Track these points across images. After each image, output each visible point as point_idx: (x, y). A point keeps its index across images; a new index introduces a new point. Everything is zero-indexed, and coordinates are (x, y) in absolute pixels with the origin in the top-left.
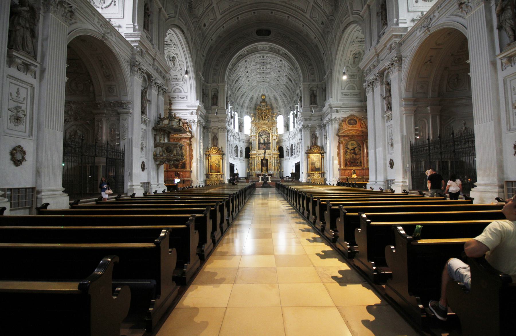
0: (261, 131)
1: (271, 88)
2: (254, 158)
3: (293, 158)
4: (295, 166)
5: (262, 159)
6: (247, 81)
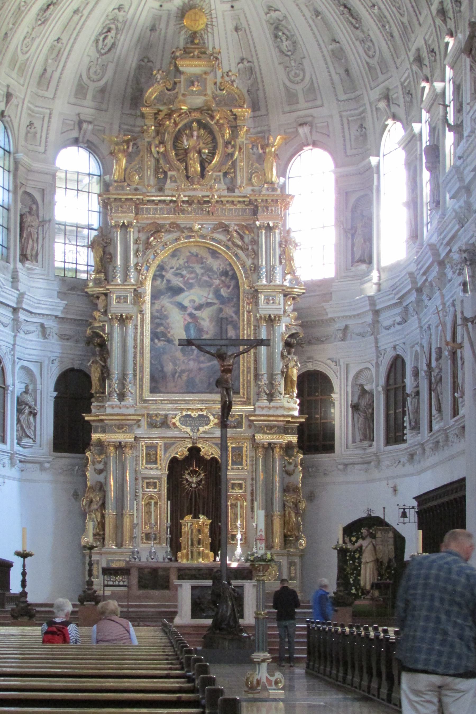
0: (174, 255)
2: (120, 447)
3: (404, 459)
4: (419, 513)
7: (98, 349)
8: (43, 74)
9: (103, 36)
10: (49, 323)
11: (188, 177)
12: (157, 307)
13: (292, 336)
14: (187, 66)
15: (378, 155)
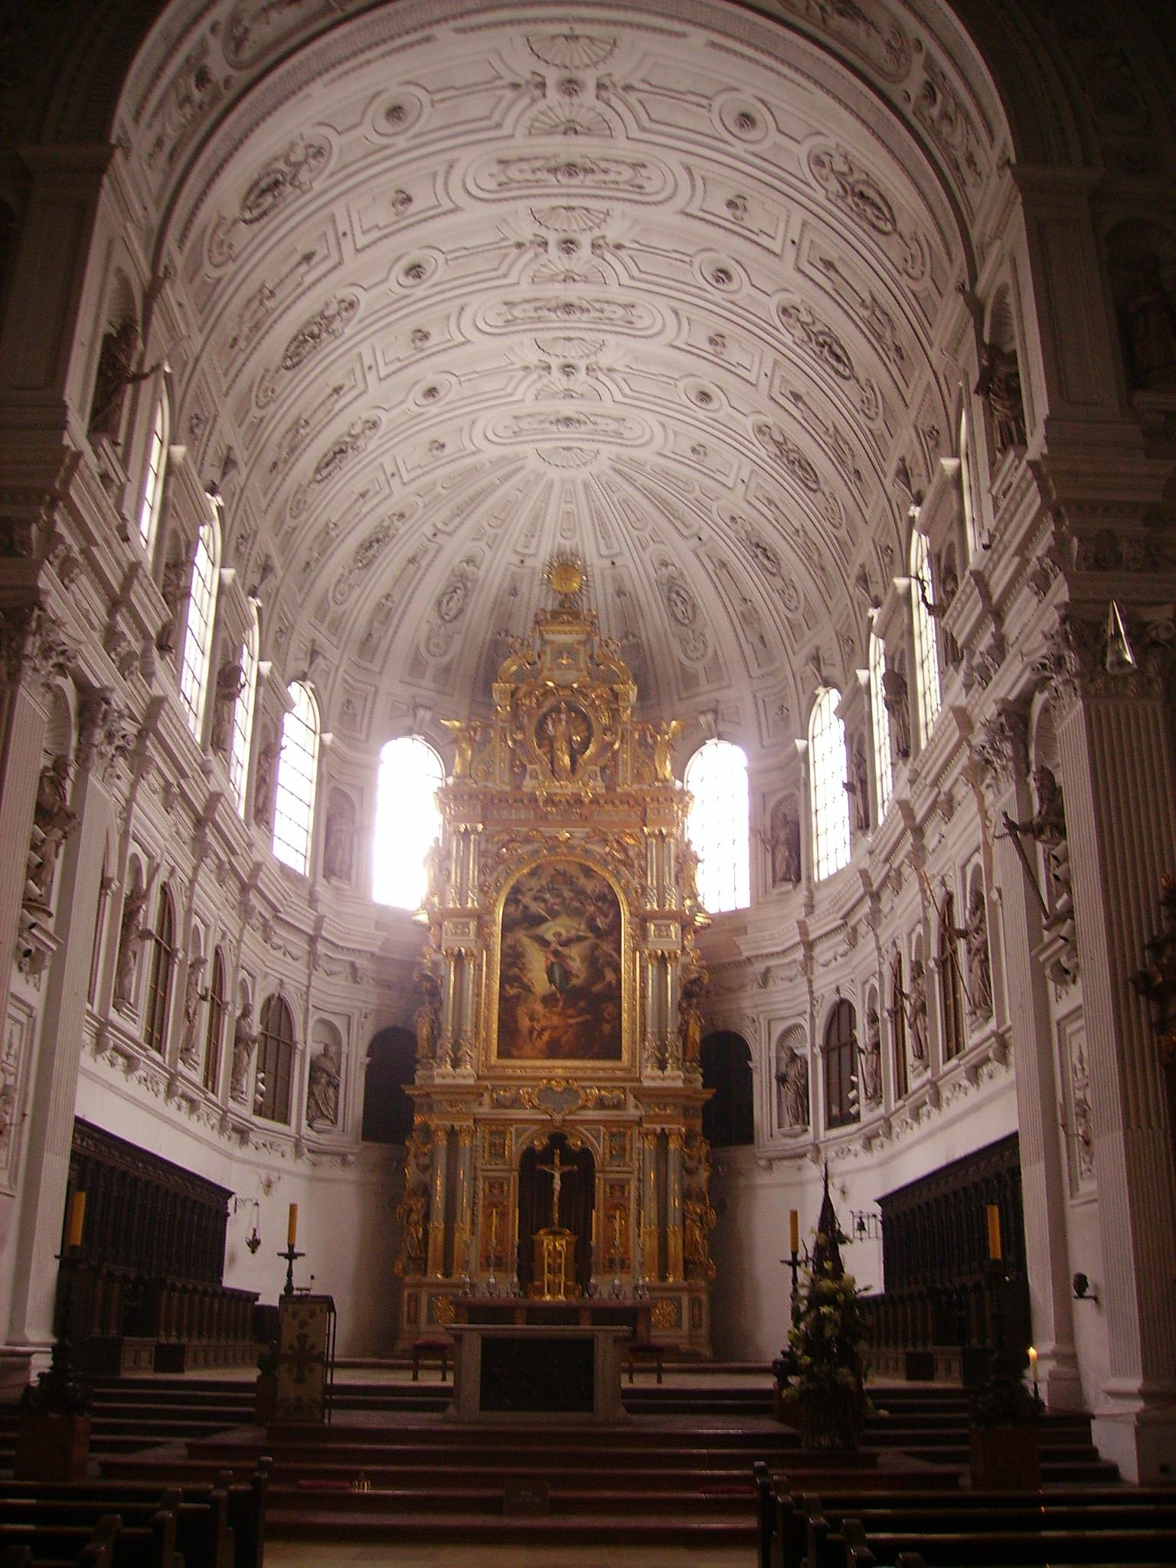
0: (533, 873)
1: (646, 492)
3: (857, 1146)
4: (886, 1224)
5: (530, 1158)
6: (417, 393)
7: (426, 998)
8: (367, 639)
9: (447, 597)
10: (362, 963)
11: (553, 772)
12: (510, 941)
13: (693, 982)
14: (553, 632)
15: (805, 737)
